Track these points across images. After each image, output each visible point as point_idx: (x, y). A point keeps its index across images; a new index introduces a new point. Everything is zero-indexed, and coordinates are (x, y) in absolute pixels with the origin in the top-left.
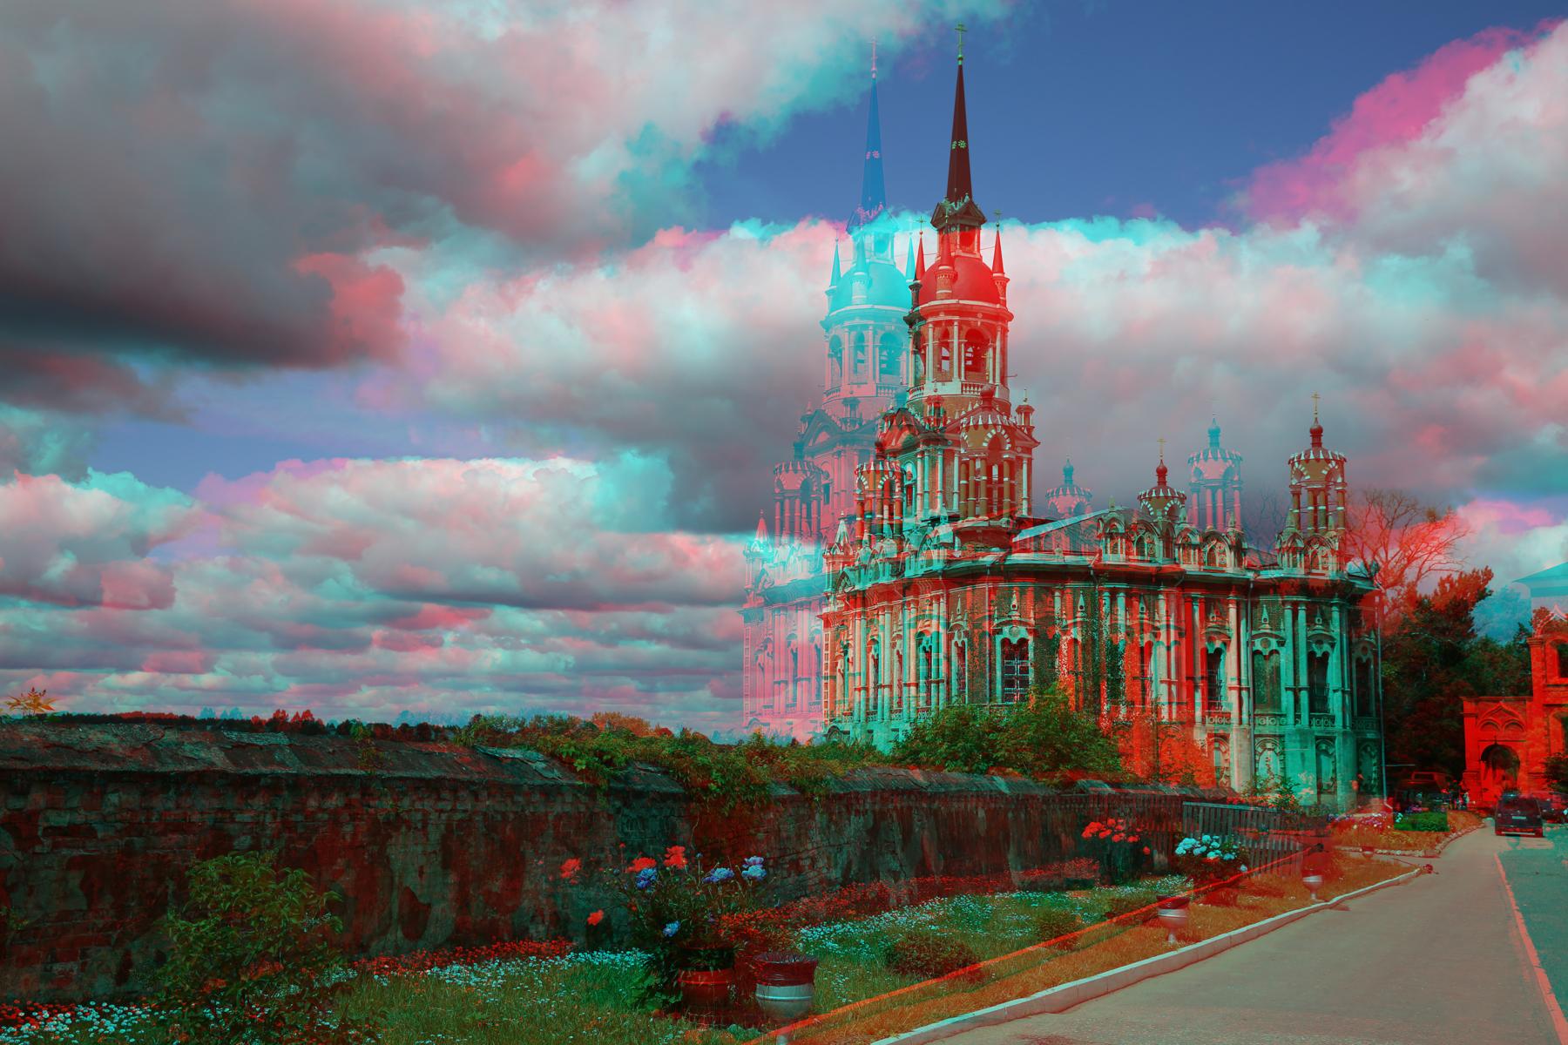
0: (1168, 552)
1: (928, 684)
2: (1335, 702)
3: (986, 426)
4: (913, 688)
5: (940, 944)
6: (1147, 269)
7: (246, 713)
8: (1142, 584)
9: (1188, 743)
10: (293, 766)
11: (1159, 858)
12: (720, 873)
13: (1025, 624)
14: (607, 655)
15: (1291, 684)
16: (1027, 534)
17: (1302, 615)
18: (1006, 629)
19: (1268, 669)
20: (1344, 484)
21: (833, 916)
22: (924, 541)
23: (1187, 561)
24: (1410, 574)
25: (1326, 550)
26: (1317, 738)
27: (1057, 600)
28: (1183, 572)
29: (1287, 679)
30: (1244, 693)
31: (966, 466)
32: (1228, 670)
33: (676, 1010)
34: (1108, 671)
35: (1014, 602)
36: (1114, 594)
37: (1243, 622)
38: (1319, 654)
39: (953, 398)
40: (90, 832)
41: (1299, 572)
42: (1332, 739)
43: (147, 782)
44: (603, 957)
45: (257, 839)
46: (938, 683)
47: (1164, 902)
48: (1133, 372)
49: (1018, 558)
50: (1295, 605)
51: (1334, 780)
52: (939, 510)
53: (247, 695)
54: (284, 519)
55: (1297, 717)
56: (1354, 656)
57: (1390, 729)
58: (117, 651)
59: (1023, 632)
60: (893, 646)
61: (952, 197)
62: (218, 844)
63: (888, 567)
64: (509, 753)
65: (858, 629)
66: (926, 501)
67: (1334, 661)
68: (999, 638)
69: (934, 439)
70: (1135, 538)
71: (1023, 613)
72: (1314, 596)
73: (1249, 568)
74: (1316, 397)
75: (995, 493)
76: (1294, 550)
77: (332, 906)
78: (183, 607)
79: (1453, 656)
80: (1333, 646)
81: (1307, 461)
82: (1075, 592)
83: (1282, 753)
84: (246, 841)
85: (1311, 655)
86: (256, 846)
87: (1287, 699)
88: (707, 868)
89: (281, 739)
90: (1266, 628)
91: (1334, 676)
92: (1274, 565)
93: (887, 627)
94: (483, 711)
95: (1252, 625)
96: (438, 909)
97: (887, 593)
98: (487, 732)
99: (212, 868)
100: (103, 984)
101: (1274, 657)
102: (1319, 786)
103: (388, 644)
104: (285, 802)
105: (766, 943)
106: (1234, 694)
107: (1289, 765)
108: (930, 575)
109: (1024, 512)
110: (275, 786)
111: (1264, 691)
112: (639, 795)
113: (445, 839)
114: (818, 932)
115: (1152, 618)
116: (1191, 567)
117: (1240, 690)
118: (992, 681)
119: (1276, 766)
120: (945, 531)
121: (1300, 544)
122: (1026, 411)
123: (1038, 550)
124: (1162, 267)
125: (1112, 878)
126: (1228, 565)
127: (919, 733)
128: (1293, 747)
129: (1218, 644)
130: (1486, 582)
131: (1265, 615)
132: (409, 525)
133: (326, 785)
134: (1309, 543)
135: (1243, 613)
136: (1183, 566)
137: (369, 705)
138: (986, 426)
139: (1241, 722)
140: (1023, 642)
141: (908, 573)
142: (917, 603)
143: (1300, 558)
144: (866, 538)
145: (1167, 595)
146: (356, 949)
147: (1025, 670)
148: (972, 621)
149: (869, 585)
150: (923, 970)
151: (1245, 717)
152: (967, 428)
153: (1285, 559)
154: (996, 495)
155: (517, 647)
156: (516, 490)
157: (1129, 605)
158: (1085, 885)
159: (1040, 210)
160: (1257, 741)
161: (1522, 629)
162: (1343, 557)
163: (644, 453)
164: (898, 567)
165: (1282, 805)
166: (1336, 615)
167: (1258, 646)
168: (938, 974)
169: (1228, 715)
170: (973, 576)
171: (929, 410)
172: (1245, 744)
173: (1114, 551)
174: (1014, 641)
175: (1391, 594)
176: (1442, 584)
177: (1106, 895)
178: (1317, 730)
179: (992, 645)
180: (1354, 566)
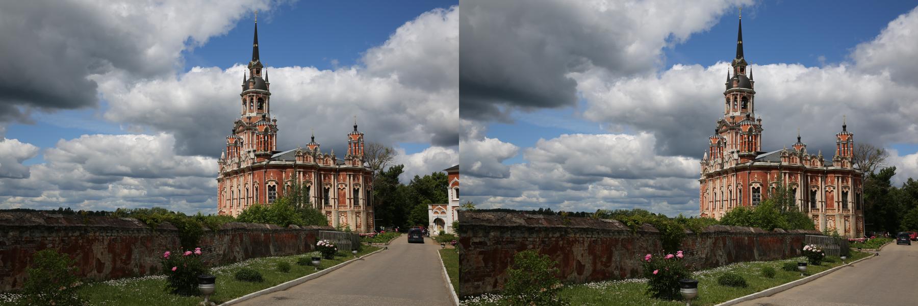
0: (315, 161)
2: (361, 202)
5: (251, 271)
6: (309, 81)
7: (50, 208)
8: (306, 169)
9: (321, 214)
10: (65, 223)
11: (312, 246)
12: (188, 252)
16: (275, 156)
21: (221, 264)
24: (381, 166)
29: (347, 196)
32: (331, 194)
33: (176, 292)
34: (301, 194)
40: (5, 244)
43: (21, 229)
44: (155, 277)
45: (54, 244)
47: (314, 259)
48: (303, 110)
49: (272, 162)
53: (51, 204)
54: (63, 152)
57: (375, 209)
58: (13, 191)
59: (274, 183)
61: (254, 60)
62: (42, 246)
64: (127, 219)
67: (360, 191)
72: (355, 172)
77: (76, 264)
78: (33, 179)
79: (393, 189)
84: (51, 245)
86: (53, 247)
88: (185, 251)
89: (61, 216)
94: (120, 207)
96: (106, 265)
98: (121, 213)
99: (40, 253)
100: (8, 288)
103: (93, 188)
104: (62, 234)
105: (201, 272)
108: (248, 167)
109: (274, 149)
110: (59, 230)
112: (165, 231)
113: (109, 244)
114: (216, 269)
116: (321, 165)
122: (275, 121)
124: (313, 81)
125: (299, 253)
126: (331, 164)
128: (349, 215)
132: (99, 154)
133: (74, 229)
137: (86, 206)
146: (82, 276)
148: (260, 180)
150: (246, 279)
153: (347, 162)
154: (266, 144)
155: (130, 189)
156: (130, 144)
158: (292, 254)
159: (280, 64)
160: (340, 213)
162: (363, 162)
163: (167, 133)
165: (347, 231)
168: (250, 281)
170: (260, 168)
175: (376, 172)
177: (296, 258)
180: (366, 164)
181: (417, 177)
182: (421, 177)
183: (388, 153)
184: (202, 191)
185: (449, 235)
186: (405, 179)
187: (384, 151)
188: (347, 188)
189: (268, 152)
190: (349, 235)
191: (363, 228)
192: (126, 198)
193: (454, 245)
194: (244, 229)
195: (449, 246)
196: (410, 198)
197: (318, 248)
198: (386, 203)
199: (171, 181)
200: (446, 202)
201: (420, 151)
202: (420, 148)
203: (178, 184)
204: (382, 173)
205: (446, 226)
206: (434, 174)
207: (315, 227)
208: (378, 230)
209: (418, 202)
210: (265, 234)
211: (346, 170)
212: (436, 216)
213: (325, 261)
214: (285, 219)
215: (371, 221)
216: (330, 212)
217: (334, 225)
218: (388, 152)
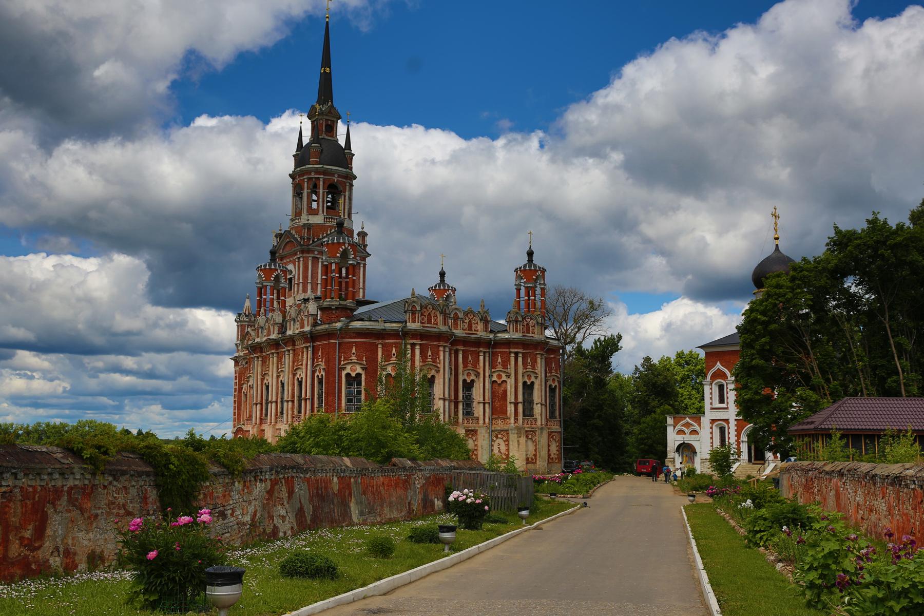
1: (300, 400)
2: (537, 409)
3: (339, 243)
4: (290, 403)
11: (438, 503)
14: (92, 384)
15: (513, 400)
17: (520, 360)
18: (349, 367)
19: (501, 391)
20: (545, 284)
22: (299, 313)
23: (456, 328)
24: (579, 337)
25: (535, 322)
26: (527, 431)
28: (454, 334)
29: (511, 397)
30: (487, 405)
31: (326, 269)
32: (477, 393)
35: (354, 351)
37: (487, 364)
38: (529, 383)
41: (518, 336)
42: (534, 432)
46: (306, 400)
48: (427, 217)
49: (357, 324)
50: (516, 354)
51: (535, 455)
52: (309, 294)
55: (516, 419)
56: (548, 384)
57: (566, 425)
60: (278, 377)
61: (320, 102)
63: (276, 328)
65: (257, 366)
66: (301, 288)
67: (536, 387)
69: (306, 251)
71: (359, 357)
73: (491, 332)
74: (530, 233)
75: (344, 285)
76: (517, 321)
80: (536, 378)
81: (525, 270)
83: (507, 440)
85: (525, 383)
87: (511, 409)
90: (500, 367)
91: (538, 395)
92: (506, 331)
93: (275, 365)
95: (493, 365)
97: (275, 344)
101: (504, 385)
102: (527, 459)
106: (482, 405)
107: (511, 447)
108: (302, 334)
111: (497, 404)
115: (435, 362)
116: (459, 332)
117: (484, 404)
119: (503, 448)
120: (312, 307)
121: (520, 319)
123: (370, 320)
126: (480, 332)
127: (294, 431)
128: (513, 437)
129: (473, 377)
130: (618, 342)
131: (499, 360)
134: (524, 318)
135: (487, 358)
136: (454, 331)
138: (339, 243)
139: (484, 423)
140: (359, 375)
141: (289, 333)
142: (294, 350)
143: (520, 327)
144: (262, 310)
145: (444, 347)
147: (359, 392)
149: (264, 339)
151: (487, 420)
152: (328, 244)
160: (494, 434)
161: (637, 368)
164: (283, 328)
165: (507, 470)
166: (539, 360)
167: (495, 378)
169: (478, 419)
170: (330, 335)
171: (305, 233)
172: (487, 436)
173: (414, 321)
174: (353, 374)
175: (569, 348)
176: (595, 343)
178: (527, 427)
179: (340, 377)
180: (549, 333)
181: (647, 360)
182: (655, 361)
183: (592, 312)
184: (202, 385)
185: (702, 476)
186: (624, 364)
187: (585, 306)
188: (511, 382)
189: (349, 303)
190: (512, 479)
191: (541, 464)
192: (17, 400)
193: (711, 495)
194: (297, 467)
195: (703, 499)
196: (632, 401)
197: (449, 507)
198: (585, 413)
199: (129, 362)
200: (700, 411)
201: (657, 307)
202: (651, 302)
203: (147, 367)
204: (579, 350)
205: (697, 460)
206: (680, 355)
207: (444, 463)
208: (569, 468)
209: (647, 410)
210: (341, 479)
211: (508, 343)
212: (680, 439)
213: (465, 534)
214: (381, 445)
215: (554, 448)
216: (475, 432)
217: (483, 458)
218: (592, 306)
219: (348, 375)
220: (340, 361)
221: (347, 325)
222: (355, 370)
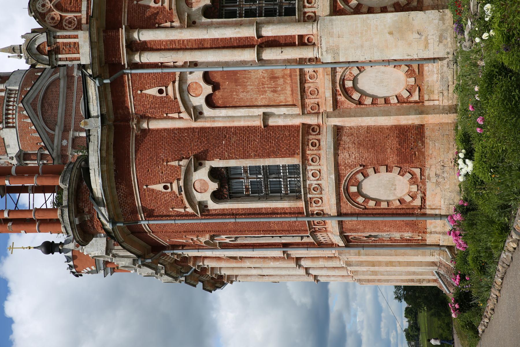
13: (187, 173)
18: (199, 197)
27: (154, 125)
35: (159, 187)
36: (135, 47)
39: (20, 137)
59: (201, 176)
68: (212, 205)
70: (56, 14)
82: (140, 99)
118: (273, 213)
140: (214, 174)
147: (254, 170)
157: (152, 22)
173: (76, 47)
174: (214, 186)
179: (223, 214)
219: (216, 196)
220: (188, 216)
221: (98, 202)
222: (205, 183)
